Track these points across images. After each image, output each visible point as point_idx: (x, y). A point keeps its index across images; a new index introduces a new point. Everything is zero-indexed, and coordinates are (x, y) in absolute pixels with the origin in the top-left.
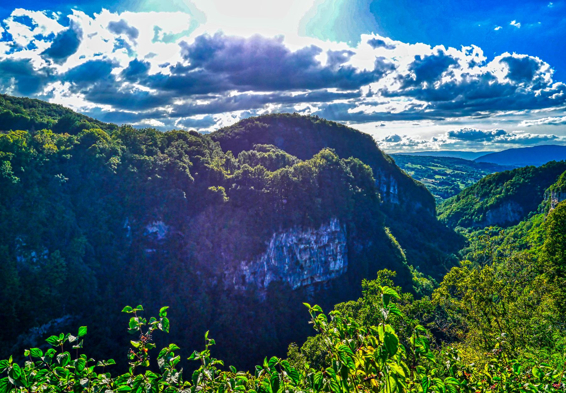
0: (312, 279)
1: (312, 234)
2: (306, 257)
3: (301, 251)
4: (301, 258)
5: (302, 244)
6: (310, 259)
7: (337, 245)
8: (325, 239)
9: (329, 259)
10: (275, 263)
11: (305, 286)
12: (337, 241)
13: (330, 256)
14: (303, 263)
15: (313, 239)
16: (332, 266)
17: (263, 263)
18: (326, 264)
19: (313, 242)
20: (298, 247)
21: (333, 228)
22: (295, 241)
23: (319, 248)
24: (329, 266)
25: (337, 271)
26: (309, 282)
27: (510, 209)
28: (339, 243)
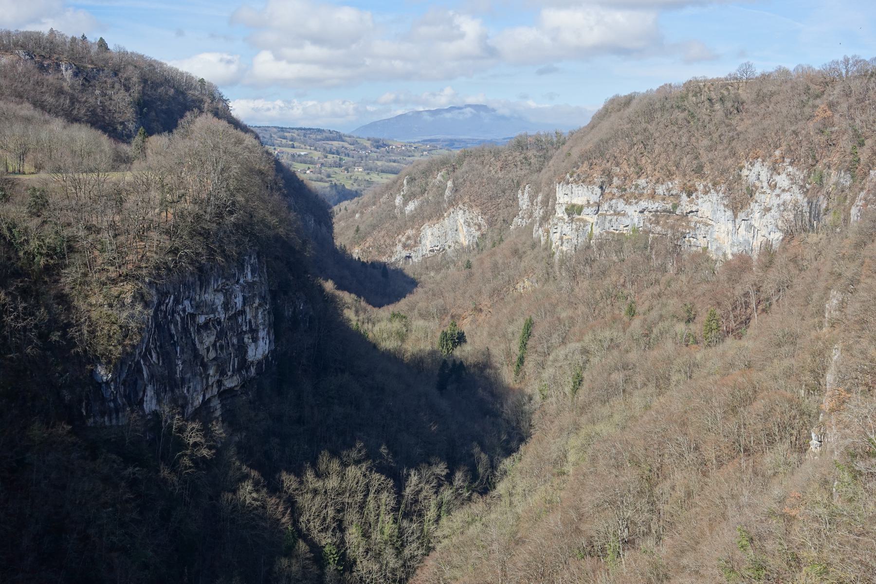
0: (220, 383)
2: (209, 339)
4: (201, 343)
6: (214, 345)
7: (257, 308)
8: (239, 301)
9: (246, 340)
10: (158, 359)
11: (209, 399)
12: (257, 301)
13: (245, 332)
15: (219, 299)
17: (139, 362)
18: (242, 349)
20: (194, 322)
22: (189, 310)
23: (230, 318)
24: (246, 352)
25: (259, 363)
26: (215, 390)
27: (462, 221)
28: (260, 305)
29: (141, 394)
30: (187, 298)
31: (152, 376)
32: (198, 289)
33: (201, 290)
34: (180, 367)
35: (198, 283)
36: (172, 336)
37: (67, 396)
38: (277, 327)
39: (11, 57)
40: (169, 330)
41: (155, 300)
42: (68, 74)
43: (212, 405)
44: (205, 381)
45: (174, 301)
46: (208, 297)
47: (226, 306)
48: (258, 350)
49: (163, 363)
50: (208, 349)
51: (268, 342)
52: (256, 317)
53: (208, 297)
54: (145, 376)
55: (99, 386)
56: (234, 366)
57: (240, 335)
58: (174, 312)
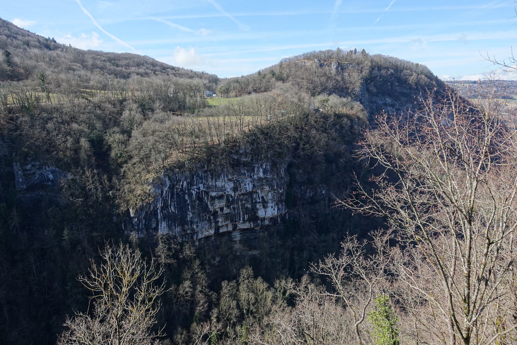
1: (230, 180)
2: (218, 204)
3: (213, 199)
9: (258, 206)
13: (259, 202)
14: (219, 210)
16: (261, 213)
20: (208, 195)
21: (261, 175)
24: (256, 213)
30: (202, 183)
31: (164, 218)
32: (210, 180)
33: (212, 179)
34: (190, 215)
36: (186, 201)
37: (115, 219)
38: (289, 200)
39: (311, 62)
40: (184, 197)
41: (168, 183)
42: (334, 67)
44: (213, 224)
45: (188, 183)
46: (219, 184)
47: (235, 189)
48: (269, 212)
50: (222, 209)
51: (276, 209)
52: (267, 195)
53: (219, 184)
54: (159, 217)
56: (244, 218)
57: (254, 204)
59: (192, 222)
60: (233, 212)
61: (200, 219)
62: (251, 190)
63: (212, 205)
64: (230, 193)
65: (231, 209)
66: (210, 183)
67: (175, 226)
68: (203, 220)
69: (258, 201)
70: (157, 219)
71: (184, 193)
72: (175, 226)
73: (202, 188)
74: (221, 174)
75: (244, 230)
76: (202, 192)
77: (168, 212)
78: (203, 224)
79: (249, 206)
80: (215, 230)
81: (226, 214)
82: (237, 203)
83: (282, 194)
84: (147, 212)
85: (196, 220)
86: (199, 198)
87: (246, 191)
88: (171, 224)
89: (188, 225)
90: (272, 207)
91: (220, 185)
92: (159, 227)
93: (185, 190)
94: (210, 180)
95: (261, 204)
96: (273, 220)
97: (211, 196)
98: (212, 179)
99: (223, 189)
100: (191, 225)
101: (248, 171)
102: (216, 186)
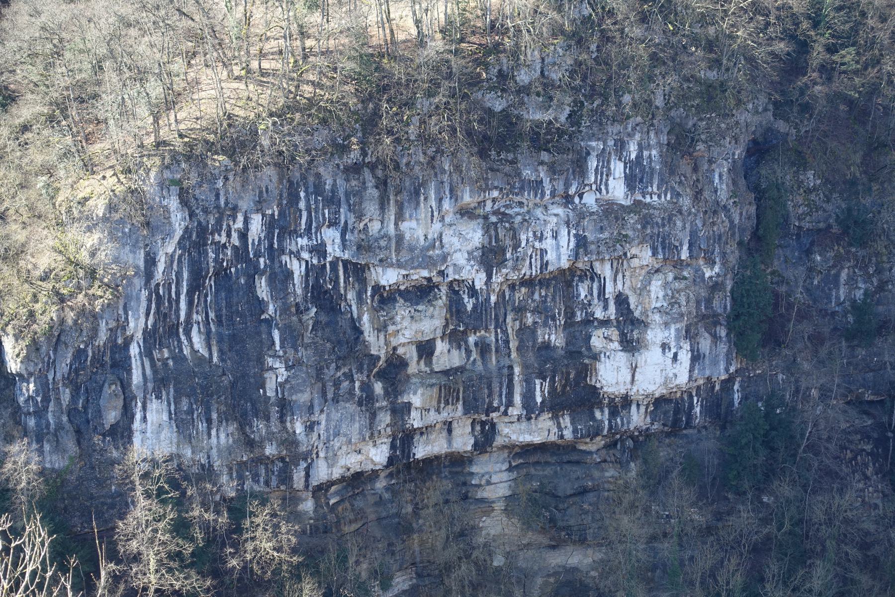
1: (466, 213)
2: (411, 327)
3: (385, 298)
5: (384, 263)
9: (597, 342)
13: (605, 323)
14: (410, 353)
16: (611, 374)
19: (460, 258)
20: (363, 282)
21: (617, 190)
24: (585, 371)
29: (112, 416)
30: (333, 224)
31: (160, 382)
32: (371, 209)
34: (277, 374)
35: (372, 192)
36: (261, 306)
38: (750, 318)
40: (251, 287)
41: (178, 221)
43: (475, 469)
44: (385, 418)
45: (270, 225)
46: (416, 229)
47: (490, 257)
48: (649, 369)
49: (221, 359)
50: (426, 349)
51: (685, 357)
53: (416, 229)
54: (136, 377)
55: (10, 380)
56: (529, 396)
57: (579, 329)
58: (273, 254)
59: (285, 407)
60: (479, 366)
61: (324, 393)
62: (565, 264)
63: (381, 328)
64: (464, 275)
65: (468, 352)
66: (375, 227)
67: (209, 421)
68: (336, 400)
69: (599, 314)
70: (125, 385)
71: (253, 272)
72: (209, 421)
73: (334, 250)
74: (424, 184)
75: (528, 450)
76: (334, 264)
77: (179, 358)
78: (336, 416)
79: (557, 339)
80: (393, 447)
81: (446, 373)
82: (500, 324)
83: (716, 287)
84: (79, 354)
85: (303, 398)
86: (323, 296)
87: (545, 265)
88: (190, 412)
89: (267, 418)
90: (665, 347)
91: (420, 233)
92: (137, 425)
93: (258, 255)
94: (371, 209)
95: (614, 333)
96: (662, 404)
97: (377, 288)
98: (383, 206)
99: (431, 254)
100: (282, 420)
101: (553, 170)
102: (400, 238)
